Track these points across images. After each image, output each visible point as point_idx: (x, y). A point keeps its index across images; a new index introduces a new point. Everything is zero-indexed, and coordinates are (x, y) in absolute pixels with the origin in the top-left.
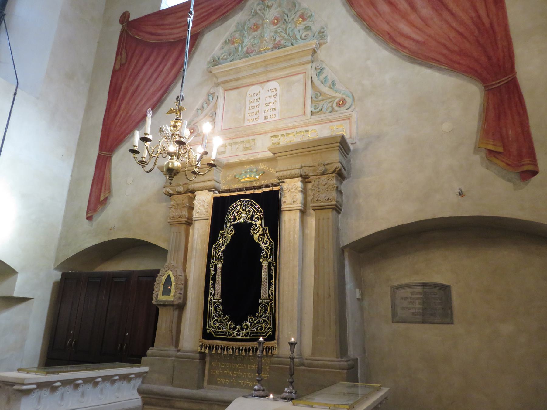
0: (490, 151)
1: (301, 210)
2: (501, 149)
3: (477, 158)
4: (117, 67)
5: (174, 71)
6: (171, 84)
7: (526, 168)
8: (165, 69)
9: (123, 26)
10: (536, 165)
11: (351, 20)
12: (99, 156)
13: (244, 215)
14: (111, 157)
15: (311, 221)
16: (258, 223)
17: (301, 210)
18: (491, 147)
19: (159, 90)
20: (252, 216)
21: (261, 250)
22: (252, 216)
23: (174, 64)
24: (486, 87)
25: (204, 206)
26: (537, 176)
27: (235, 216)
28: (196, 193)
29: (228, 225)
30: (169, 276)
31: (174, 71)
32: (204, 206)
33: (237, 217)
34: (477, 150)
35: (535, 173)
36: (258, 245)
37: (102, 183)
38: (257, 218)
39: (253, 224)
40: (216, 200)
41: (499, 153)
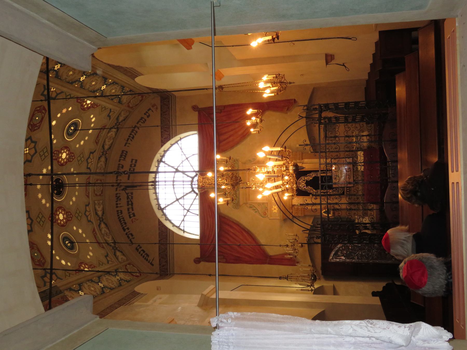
0: (287, 110)
1: (302, 164)
2: (287, 108)
3: (289, 113)
4: (225, 260)
5: (235, 226)
6: (240, 227)
7: (293, 101)
8: (232, 231)
9: (202, 261)
10: (293, 99)
11: (232, 150)
12: (270, 263)
13: (303, 184)
14: (271, 256)
15: (306, 160)
16: (306, 178)
17: (302, 164)
18: (286, 110)
19: (243, 233)
20: (303, 180)
21: (315, 176)
22: (303, 180)
23: (231, 227)
24: (267, 110)
25: (298, 200)
26: (296, 99)
27: (303, 187)
28: (293, 204)
29: (306, 189)
30: (324, 212)
31: (235, 226)
32: (298, 200)
33: (304, 186)
34: (286, 113)
35: (295, 100)
36: (314, 178)
37: (282, 259)
38: (304, 179)
39: (306, 180)
40: (297, 195)
41: (288, 108)
